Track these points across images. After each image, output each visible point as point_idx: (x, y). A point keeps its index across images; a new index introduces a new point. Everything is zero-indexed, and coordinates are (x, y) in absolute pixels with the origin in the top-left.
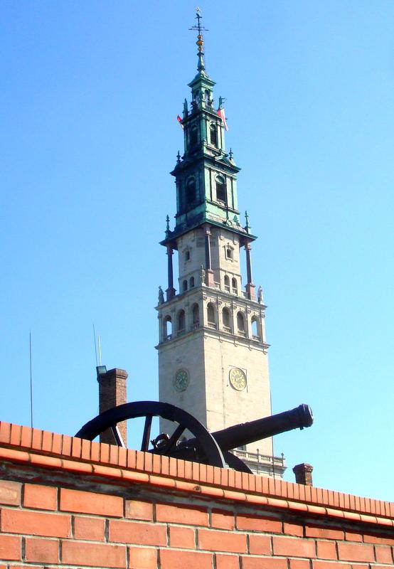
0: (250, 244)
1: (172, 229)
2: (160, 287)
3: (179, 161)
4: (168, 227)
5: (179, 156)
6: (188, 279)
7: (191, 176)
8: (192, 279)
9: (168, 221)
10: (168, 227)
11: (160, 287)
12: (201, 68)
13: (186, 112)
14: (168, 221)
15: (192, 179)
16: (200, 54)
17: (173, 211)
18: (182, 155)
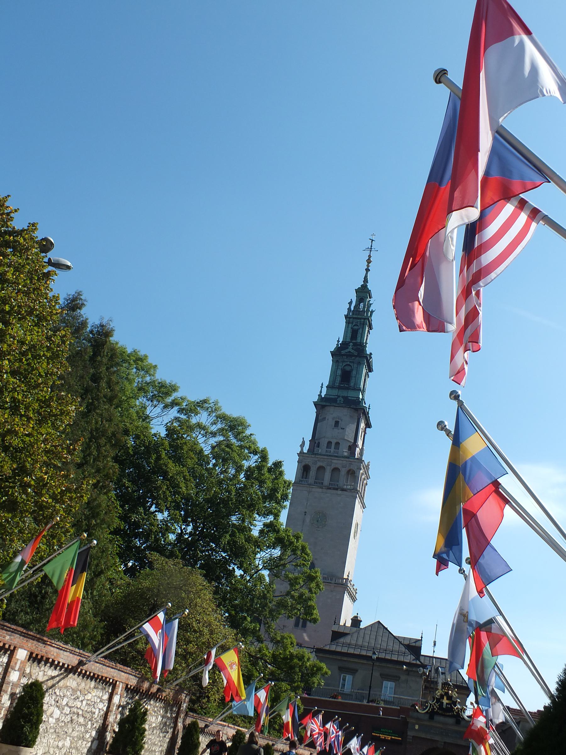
0: (367, 429)
1: (323, 396)
2: (303, 438)
3: (337, 345)
4: (321, 392)
5: (338, 341)
6: (334, 442)
7: (348, 363)
8: (337, 444)
9: (322, 387)
10: (321, 392)
11: (303, 438)
12: (366, 280)
13: (349, 309)
14: (322, 387)
15: (349, 365)
16: (367, 270)
17: (326, 383)
18: (341, 342)
